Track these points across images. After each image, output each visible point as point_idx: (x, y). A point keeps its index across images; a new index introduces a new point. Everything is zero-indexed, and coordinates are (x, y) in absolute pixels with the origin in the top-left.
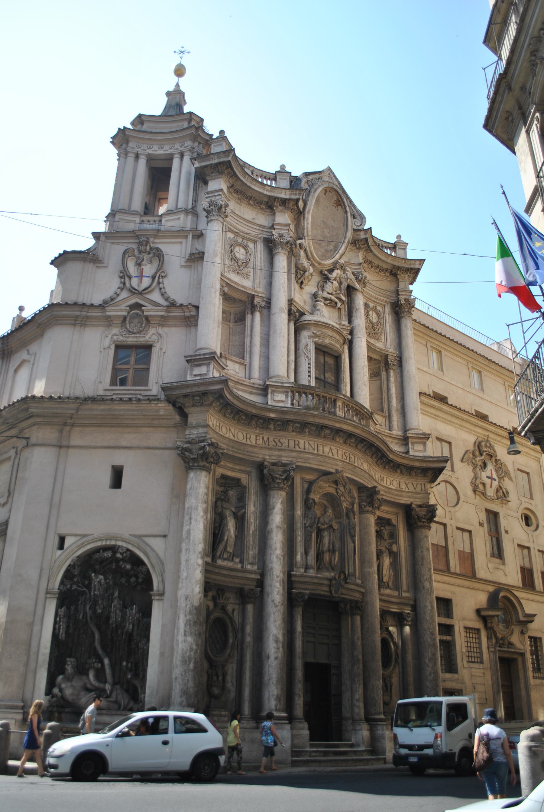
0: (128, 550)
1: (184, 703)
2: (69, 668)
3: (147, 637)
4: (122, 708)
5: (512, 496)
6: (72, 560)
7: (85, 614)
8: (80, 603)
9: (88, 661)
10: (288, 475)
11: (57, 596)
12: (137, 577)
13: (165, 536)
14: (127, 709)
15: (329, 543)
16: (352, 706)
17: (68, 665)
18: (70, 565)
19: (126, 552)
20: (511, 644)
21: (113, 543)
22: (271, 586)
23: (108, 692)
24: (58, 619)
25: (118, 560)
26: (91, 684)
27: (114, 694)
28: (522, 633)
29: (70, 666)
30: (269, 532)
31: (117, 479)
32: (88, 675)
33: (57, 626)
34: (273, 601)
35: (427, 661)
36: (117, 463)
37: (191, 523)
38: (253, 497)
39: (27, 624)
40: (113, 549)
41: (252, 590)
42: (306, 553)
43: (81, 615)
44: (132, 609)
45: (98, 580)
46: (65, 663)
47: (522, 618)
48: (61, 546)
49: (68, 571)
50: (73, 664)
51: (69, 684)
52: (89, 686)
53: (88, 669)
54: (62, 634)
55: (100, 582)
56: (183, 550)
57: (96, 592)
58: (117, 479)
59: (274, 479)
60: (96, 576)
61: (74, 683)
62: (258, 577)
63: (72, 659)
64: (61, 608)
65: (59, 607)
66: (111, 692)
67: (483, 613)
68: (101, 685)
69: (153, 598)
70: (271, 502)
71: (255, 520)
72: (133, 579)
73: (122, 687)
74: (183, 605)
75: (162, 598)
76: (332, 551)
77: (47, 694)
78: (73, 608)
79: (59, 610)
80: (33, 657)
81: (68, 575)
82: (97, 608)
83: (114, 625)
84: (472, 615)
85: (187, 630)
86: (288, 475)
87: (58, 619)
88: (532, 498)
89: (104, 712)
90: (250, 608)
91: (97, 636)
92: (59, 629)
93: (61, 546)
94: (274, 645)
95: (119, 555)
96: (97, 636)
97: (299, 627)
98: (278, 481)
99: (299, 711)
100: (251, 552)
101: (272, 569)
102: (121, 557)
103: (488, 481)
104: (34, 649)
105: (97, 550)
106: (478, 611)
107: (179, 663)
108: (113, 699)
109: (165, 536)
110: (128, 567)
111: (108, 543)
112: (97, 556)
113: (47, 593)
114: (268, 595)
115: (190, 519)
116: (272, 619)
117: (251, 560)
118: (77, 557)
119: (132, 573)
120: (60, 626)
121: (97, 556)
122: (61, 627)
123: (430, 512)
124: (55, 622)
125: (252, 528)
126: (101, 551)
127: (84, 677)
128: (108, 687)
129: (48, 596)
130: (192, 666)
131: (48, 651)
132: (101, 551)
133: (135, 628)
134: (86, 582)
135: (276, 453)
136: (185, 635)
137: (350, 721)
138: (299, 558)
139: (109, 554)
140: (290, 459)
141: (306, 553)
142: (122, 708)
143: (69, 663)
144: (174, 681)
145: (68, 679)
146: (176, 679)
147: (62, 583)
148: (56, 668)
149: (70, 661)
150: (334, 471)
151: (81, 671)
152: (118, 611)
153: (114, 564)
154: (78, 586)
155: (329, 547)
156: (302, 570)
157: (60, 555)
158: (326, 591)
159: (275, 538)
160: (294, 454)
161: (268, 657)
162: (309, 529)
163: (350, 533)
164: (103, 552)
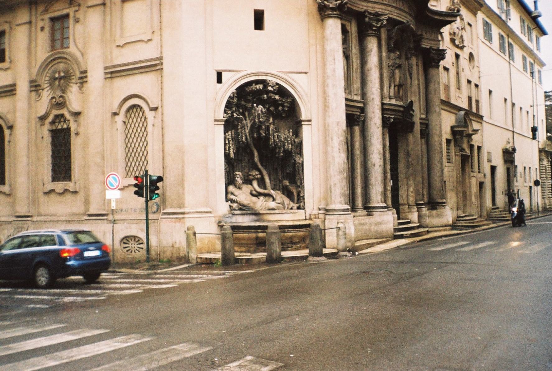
0: (277, 84)
1: (343, 202)
2: (239, 180)
3: (301, 153)
5: (465, 44)
6: (233, 93)
7: (246, 136)
8: (239, 128)
9: (250, 173)
10: (382, 23)
11: (223, 123)
12: (283, 106)
13: (306, 73)
15: (400, 78)
16: (408, 196)
18: (230, 97)
19: (275, 86)
20: (464, 150)
21: (264, 78)
22: (373, 112)
25: (268, 92)
26: (255, 190)
28: (468, 142)
30: (368, 70)
31: (259, 20)
32: (251, 184)
33: (227, 147)
34: (375, 124)
35: (437, 163)
36: (259, 8)
37: (335, 63)
38: (354, 41)
40: (264, 82)
41: (359, 115)
42: (390, 87)
43: (244, 138)
44: (289, 132)
45: (260, 109)
47: (471, 132)
48: (219, 80)
49: (228, 102)
51: (241, 192)
52: (254, 192)
53: (253, 179)
55: (262, 111)
56: (330, 85)
57: (261, 119)
58: (259, 20)
59: (371, 26)
60: (257, 106)
62: (362, 106)
63: (240, 173)
64: (227, 132)
65: (225, 132)
67: (456, 129)
69: (303, 123)
70: (369, 46)
71: (357, 60)
72: (280, 108)
74: (336, 129)
75: (310, 123)
76: (400, 86)
77: (227, 201)
78: (233, 132)
79: (227, 134)
81: (229, 105)
82: (261, 132)
84: (448, 130)
85: (341, 148)
86: (382, 23)
87: (227, 142)
88: (472, 44)
89: (277, 211)
90: (357, 129)
91: (256, 154)
92: (229, 150)
93: (219, 80)
94: (379, 156)
95: (270, 88)
96: (256, 154)
97: (388, 144)
98: (374, 28)
99: (390, 202)
100: (355, 86)
101: (373, 99)
102: (272, 90)
103: (456, 31)
105: (250, 83)
106: (452, 127)
107: (336, 173)
109: (306, 73)
110: (277, 97)
111: (260, 78)
112: (248, 89)
114: (371, 119)
115: (334, 59)
116: (375, 138)
117: (355, 92)
118: (236, 89)
119: (280, 102)
120: (229, 147)
121: (248, 89)
122: (231, 149)
123: (441, 55)
124: (225, 144)
125: (355, 67)
126: (254, 85)
127: (249, 186)
129: (217, 123)
130: (345, 174)
131: (223, 167)
132: (254, 85)
134: (241, 111)
135: (370, 5)
136: (339, 152)
137: (407, 206)
138: (385, 90)
139: (260, 87)
140: (381, 10)
141: (390, 87)
144: (332, 187)
145: (240, 188)
146: (335, 185)
147: (225, 112)
148: (230, 181)
150: (405, 21)
151: (247, 181)
152: (275, 134)
153: (265, 96)
154: (238, 115)
155: (399, 82)
156: (388, 100)
157: (220, 89)
158: (400, 116)
159: (374, 75)
160: (383, 7)
161: (374, 165)
162: (391, 68)
163: (409, 71)
164: (256, 85)
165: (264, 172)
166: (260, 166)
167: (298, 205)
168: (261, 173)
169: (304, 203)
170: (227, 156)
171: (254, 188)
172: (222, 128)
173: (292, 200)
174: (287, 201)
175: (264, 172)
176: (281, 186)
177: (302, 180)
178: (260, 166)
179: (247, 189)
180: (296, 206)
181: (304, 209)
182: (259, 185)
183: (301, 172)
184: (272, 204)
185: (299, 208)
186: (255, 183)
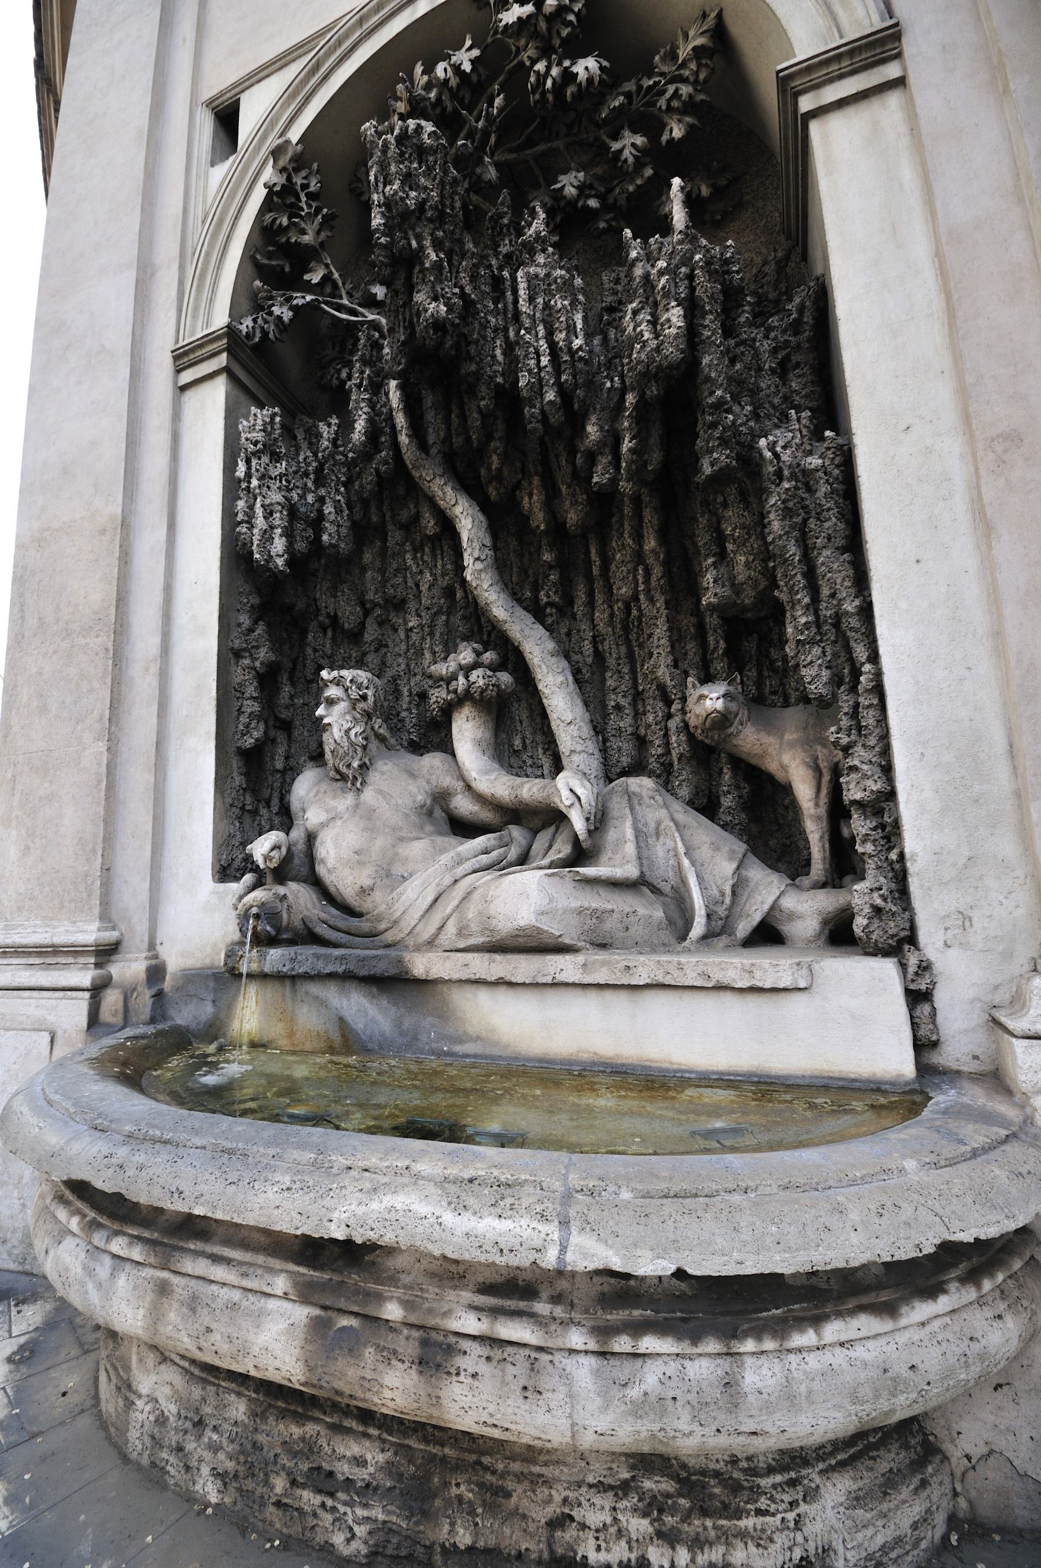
2: (338, 721)
4: (698, 929)
14: (743, 928)
17: (331, 702)
23: (579, 824)
24: (241, 470)
27: (622, 833)
29: (343, 706)
39: (103, 531)
46: (313, 689)
49: (265, 233)
50: (354, 694)
51: (344, 802)
52: (464, 806)
53: (448, 711)
54: (267, 537)
61: (368, 795)
66: (599, 821)
68: (530, 790)
73: (665, 778)
80: (143, 685)
83: (550, 395)
91: (468, 522)
104: (144, 642)
108: (619, 861)
113: (183, 359)
124: (232, 488)
127: (432, 762)
128: (572, 790)
133: (710, 326)
142: (698, 929)
143: (333, 691)
147: (249, 300)
149: (338, 682)
165: (536, 645)
166: (498, 606)
167: (826, 901)
168: (513, 659)
169: (899, 877)
170: (237, 558)
171: (462, 777)
172: (217, 392)
173: (783, 853)
174: (708, 860)
175: (536, 645)
176: (678, 744)
177: (851, 635)
178: (498, 606)
179: (399, 784)
180: (807, 908)
181: (901, 944)
182: (505, 753)
183: (831, 565)
184: (527, 896)
185: (839, 934)
186: (467, 733)
